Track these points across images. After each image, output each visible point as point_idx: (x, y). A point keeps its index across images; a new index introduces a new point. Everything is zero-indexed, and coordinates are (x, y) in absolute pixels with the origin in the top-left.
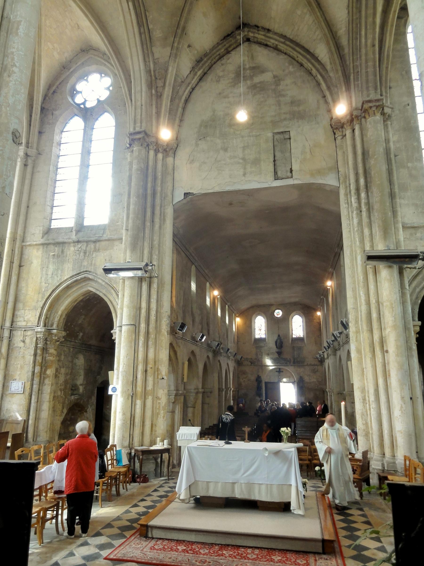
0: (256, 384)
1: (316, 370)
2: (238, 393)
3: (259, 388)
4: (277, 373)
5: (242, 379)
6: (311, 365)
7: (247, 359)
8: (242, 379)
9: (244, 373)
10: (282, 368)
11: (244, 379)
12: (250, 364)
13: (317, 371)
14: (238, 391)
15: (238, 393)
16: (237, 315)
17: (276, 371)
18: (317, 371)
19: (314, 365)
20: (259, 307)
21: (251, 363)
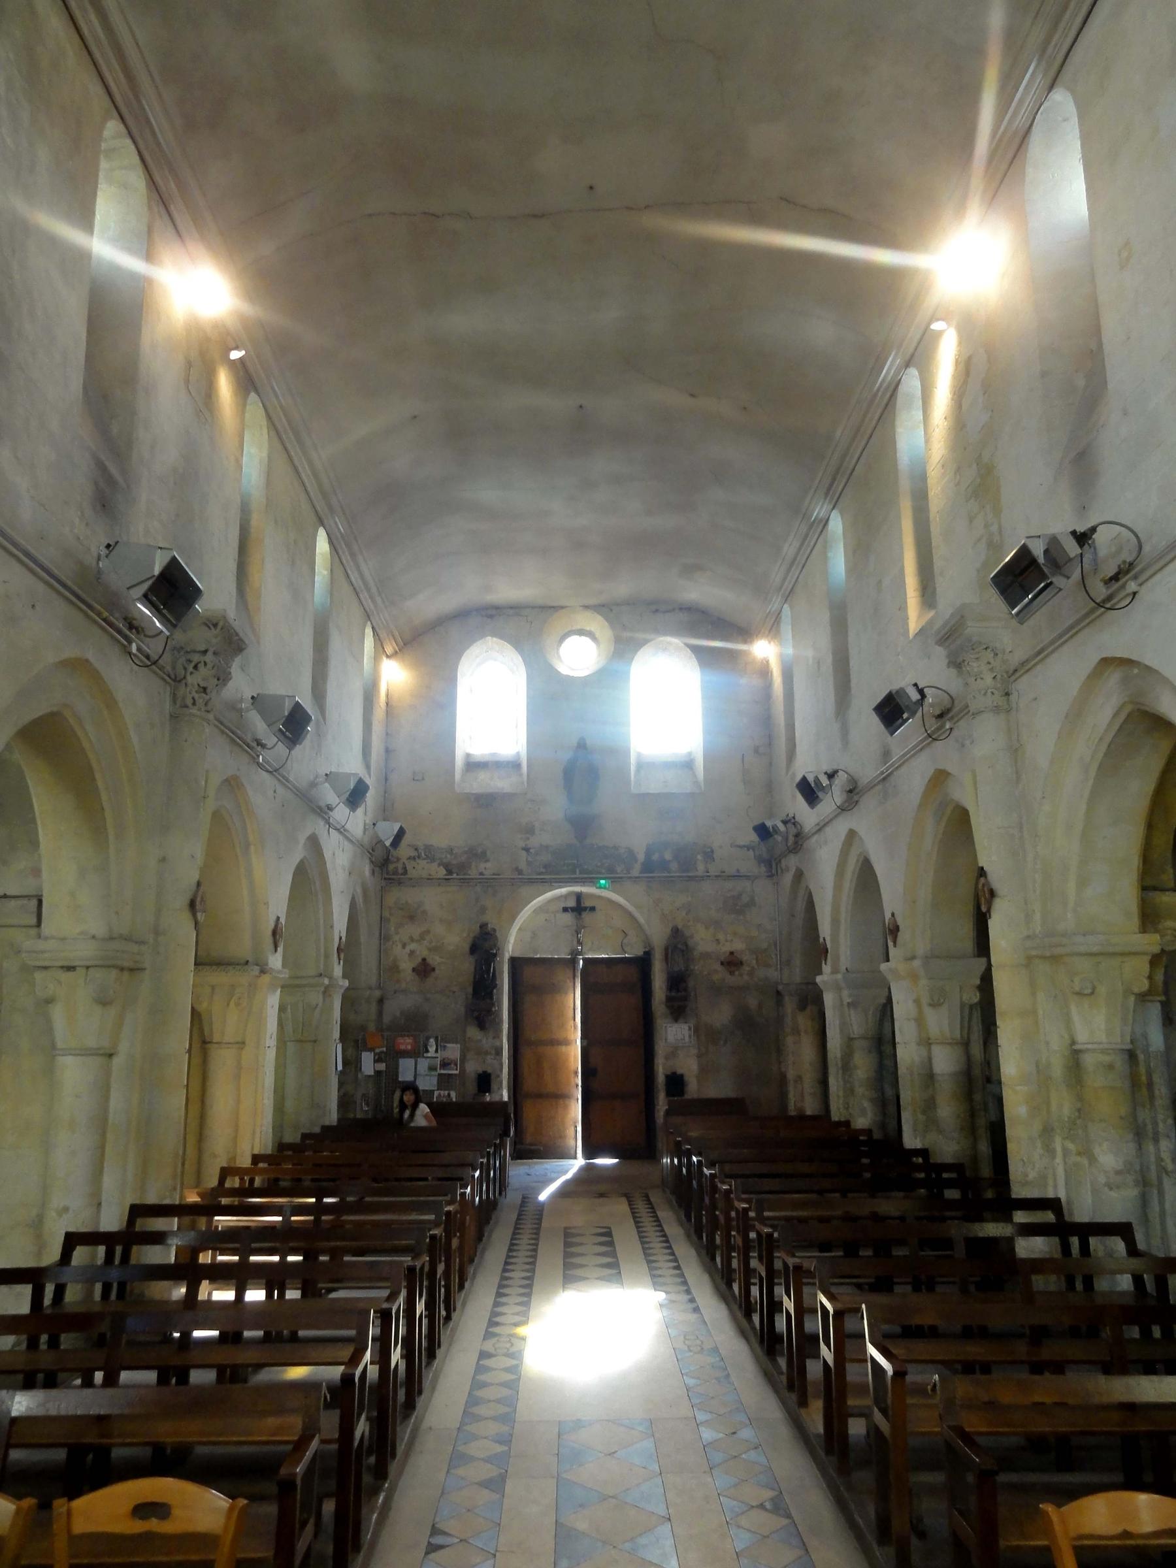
0: (467, 966)
1: (745, 899)
2: (380, 1013)
3: (483, 986)
4: (568, 918)
5: (404, 946)
6: (723, 876)
7: (429, 854)
8: (404, 946)
9: (412, 915)
10: (592, 896)
11: (413, 946)
12: (442, 872)
13: (752, 903)
14: (381, 1001)
15: (380, 1013)
16: (389, 650)
17: (565, 910)
18: (752, 903)
19: (738, 876)
20: (491, 617)
21: (450, 872)
